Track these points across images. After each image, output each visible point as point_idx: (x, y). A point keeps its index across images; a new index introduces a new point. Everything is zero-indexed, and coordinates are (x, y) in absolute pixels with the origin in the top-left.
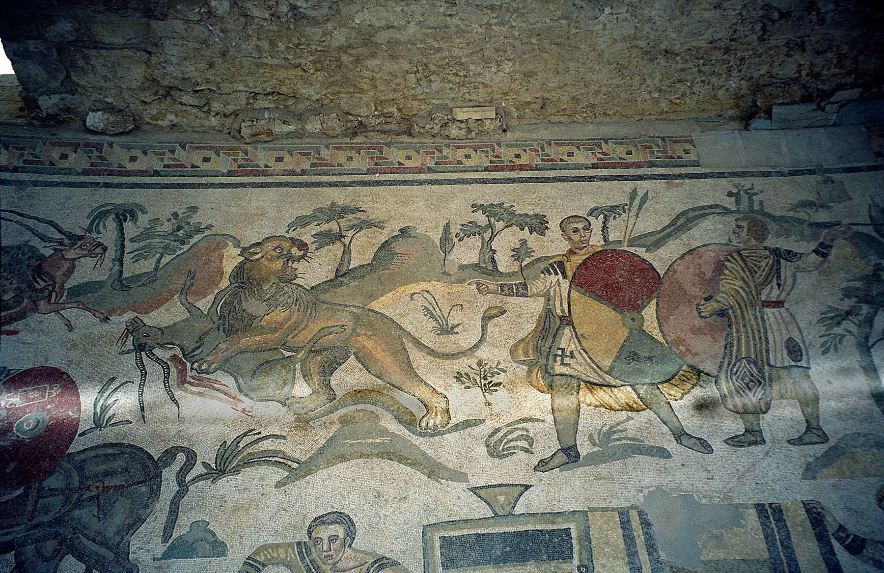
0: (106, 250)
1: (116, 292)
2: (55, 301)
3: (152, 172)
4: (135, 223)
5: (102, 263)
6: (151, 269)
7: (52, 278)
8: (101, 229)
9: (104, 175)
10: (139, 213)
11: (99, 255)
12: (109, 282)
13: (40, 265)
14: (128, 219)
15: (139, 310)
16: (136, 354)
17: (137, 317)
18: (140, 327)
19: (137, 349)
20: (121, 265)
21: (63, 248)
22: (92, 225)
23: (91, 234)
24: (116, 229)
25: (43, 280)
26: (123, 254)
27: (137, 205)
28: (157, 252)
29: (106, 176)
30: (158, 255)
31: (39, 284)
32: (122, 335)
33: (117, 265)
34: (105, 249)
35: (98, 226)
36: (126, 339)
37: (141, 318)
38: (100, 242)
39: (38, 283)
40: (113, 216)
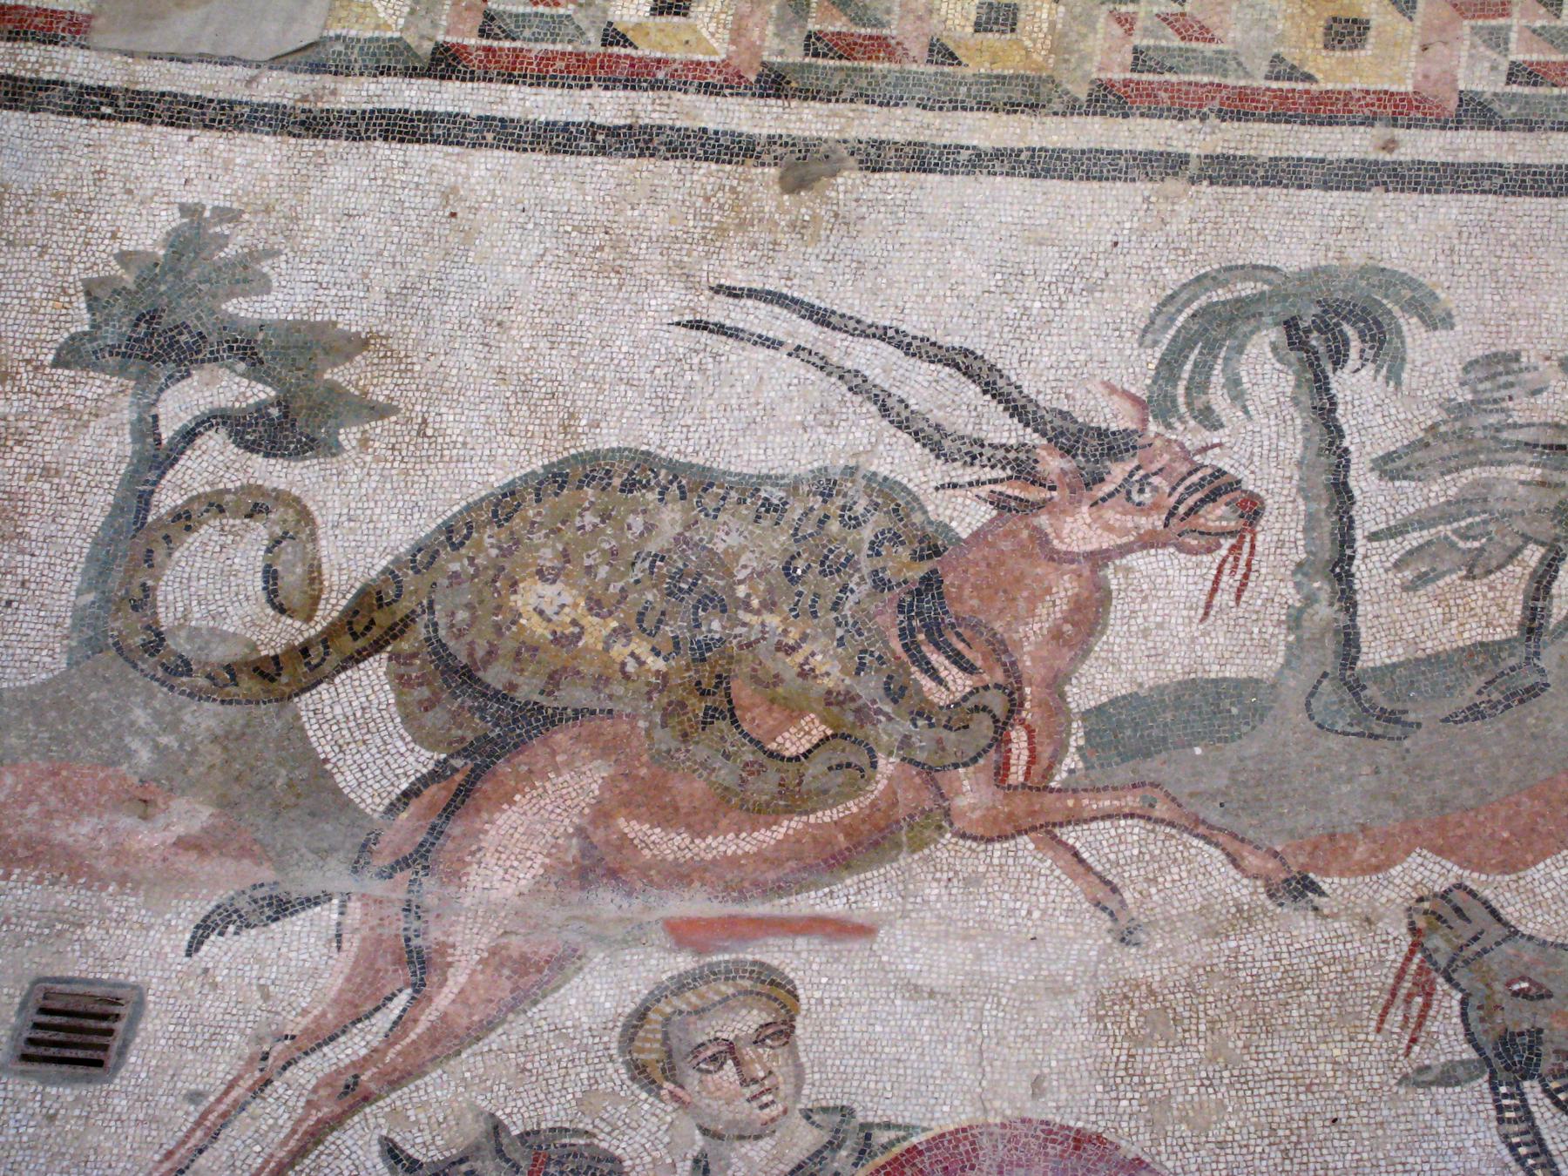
0: (1257, 514)
1: (1334, 743)
2: (1027, 774)
3: (1453, 105)
4: (1394, 375)
5: (1243, 585)
6: (1505, 627)
7: (999, 648)
8: (1219, 399)
9: (1204, 118)
10: (1410, 326)
11: (1230, 542)
12: (1296, 685)
13: (931, 582)
14: (1354, 354)
15: (1471, 848)
16: (1494, 1088)
17: (1460, 886)
18: (1486, 940)
19: (1498, 1064)
20: (1347, 598)
21: (1035, 494)
22: (1173, 379)
23: (1169, 426)
24: (1295, 401)
25: (957, 659)
26: (1345, 539)
27: (1390, 280)
28: (1527, 539)
29: (1213, 120)
30: (1533, 555)
31: (940, 681)
32: (1400, 977)
33: (1324, 596)
34: (1251, 509)
35: (1199, 385)
36: (1427, 1006)
37: (1487, 893)
38: (1220, 473)
39: (933, 673)
40: (1275, 334)
